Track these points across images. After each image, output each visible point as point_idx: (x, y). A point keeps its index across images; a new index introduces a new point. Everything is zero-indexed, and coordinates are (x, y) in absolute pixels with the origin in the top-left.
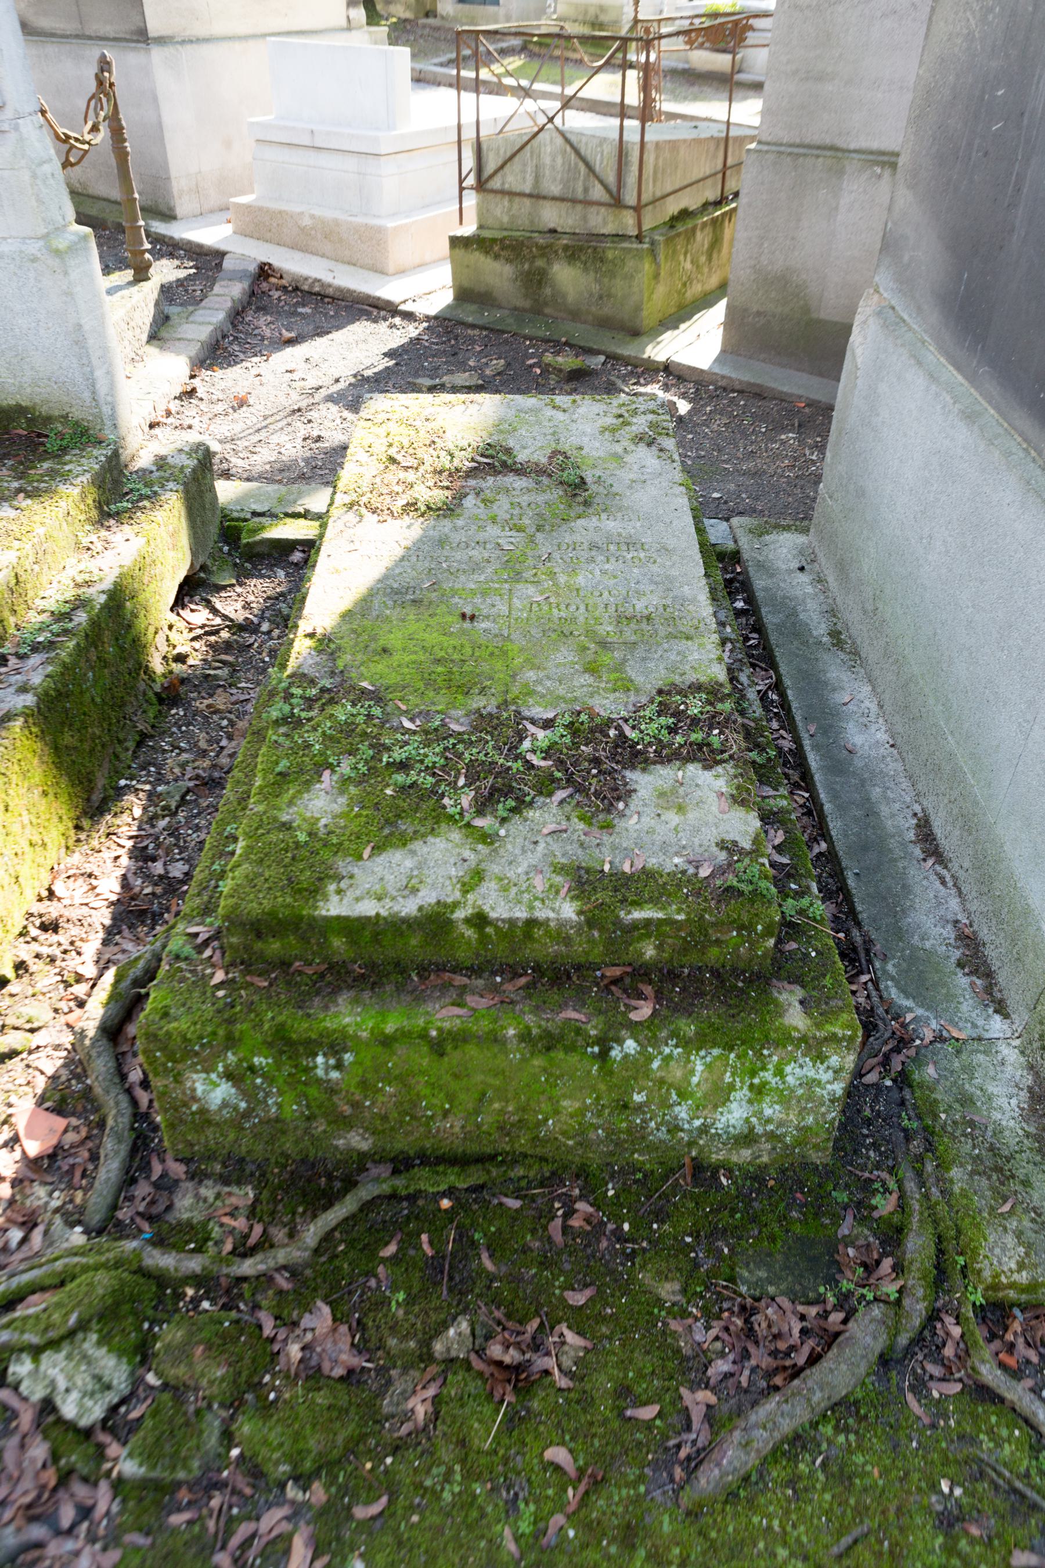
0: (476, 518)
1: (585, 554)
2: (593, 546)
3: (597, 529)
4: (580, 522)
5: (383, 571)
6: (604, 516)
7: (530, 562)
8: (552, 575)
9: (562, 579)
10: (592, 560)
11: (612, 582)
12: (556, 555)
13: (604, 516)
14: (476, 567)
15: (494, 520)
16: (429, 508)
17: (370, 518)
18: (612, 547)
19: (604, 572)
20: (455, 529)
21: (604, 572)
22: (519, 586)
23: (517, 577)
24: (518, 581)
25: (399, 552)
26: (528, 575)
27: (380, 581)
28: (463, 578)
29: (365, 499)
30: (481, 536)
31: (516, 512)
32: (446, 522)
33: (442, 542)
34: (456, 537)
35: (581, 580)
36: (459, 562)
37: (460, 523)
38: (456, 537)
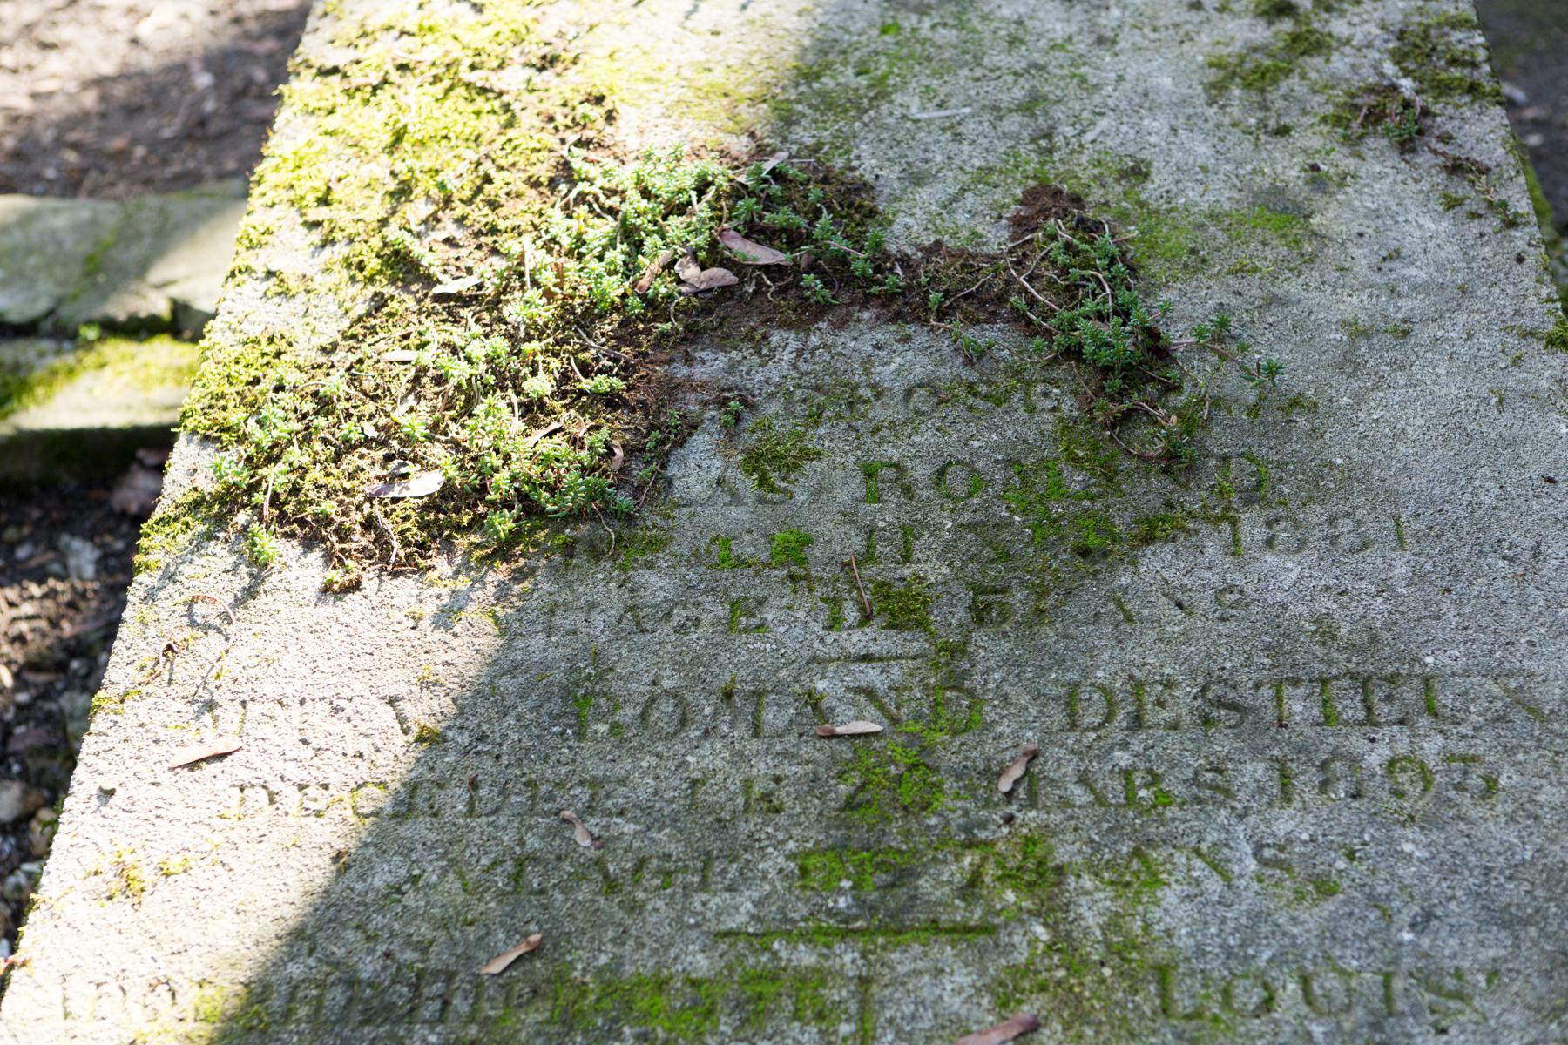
0: (721, 556)
1: (1182, 754)
2: (1219, 706)
3: (1229, 601)
4: (1159, 563)
5: (320, 872)
6: (1252, 527)
7: (952, 806)
8: (1043, 879)
9: (1092, 907)
10: (1213, 787)
11: (1314, 916)
12: (1061, 765)
13: (1252, 527)
14: (714, 841)
15: (794, 561)
16: (531, 508)
17: (299, 570)
18: (1298, 706)
19: (1273, 858)
20: (636, 620)
21: (1273, 858)
22: (903, 960)
23: (891, 917)
24: (896, 928)
25: (395, 758)
26: (938, 884)
27: (300, 938)
28: (658, 911)
29: (276, 476)
30: (745, 659)
31: (886, 516)
32: (599, 585)
33: (577, 698)
34: (644, 668)
35: (1171, 910)
36: (648, 814)
37: (657, 583)
38: (644, 668)
